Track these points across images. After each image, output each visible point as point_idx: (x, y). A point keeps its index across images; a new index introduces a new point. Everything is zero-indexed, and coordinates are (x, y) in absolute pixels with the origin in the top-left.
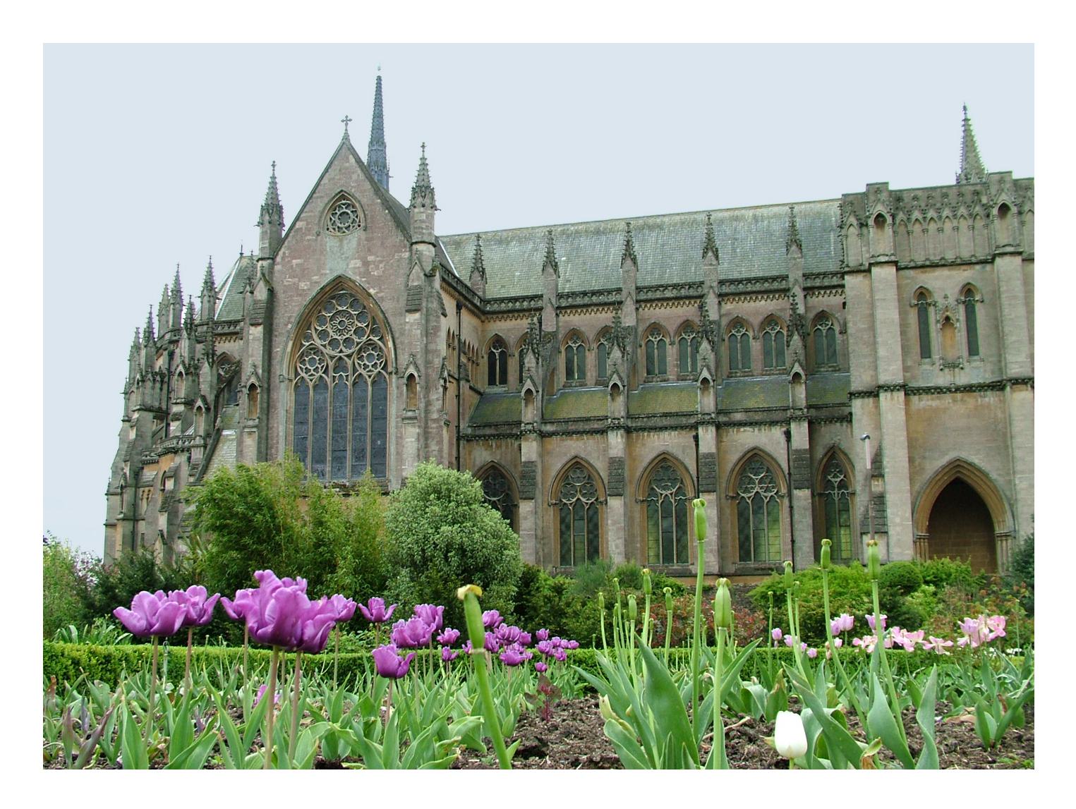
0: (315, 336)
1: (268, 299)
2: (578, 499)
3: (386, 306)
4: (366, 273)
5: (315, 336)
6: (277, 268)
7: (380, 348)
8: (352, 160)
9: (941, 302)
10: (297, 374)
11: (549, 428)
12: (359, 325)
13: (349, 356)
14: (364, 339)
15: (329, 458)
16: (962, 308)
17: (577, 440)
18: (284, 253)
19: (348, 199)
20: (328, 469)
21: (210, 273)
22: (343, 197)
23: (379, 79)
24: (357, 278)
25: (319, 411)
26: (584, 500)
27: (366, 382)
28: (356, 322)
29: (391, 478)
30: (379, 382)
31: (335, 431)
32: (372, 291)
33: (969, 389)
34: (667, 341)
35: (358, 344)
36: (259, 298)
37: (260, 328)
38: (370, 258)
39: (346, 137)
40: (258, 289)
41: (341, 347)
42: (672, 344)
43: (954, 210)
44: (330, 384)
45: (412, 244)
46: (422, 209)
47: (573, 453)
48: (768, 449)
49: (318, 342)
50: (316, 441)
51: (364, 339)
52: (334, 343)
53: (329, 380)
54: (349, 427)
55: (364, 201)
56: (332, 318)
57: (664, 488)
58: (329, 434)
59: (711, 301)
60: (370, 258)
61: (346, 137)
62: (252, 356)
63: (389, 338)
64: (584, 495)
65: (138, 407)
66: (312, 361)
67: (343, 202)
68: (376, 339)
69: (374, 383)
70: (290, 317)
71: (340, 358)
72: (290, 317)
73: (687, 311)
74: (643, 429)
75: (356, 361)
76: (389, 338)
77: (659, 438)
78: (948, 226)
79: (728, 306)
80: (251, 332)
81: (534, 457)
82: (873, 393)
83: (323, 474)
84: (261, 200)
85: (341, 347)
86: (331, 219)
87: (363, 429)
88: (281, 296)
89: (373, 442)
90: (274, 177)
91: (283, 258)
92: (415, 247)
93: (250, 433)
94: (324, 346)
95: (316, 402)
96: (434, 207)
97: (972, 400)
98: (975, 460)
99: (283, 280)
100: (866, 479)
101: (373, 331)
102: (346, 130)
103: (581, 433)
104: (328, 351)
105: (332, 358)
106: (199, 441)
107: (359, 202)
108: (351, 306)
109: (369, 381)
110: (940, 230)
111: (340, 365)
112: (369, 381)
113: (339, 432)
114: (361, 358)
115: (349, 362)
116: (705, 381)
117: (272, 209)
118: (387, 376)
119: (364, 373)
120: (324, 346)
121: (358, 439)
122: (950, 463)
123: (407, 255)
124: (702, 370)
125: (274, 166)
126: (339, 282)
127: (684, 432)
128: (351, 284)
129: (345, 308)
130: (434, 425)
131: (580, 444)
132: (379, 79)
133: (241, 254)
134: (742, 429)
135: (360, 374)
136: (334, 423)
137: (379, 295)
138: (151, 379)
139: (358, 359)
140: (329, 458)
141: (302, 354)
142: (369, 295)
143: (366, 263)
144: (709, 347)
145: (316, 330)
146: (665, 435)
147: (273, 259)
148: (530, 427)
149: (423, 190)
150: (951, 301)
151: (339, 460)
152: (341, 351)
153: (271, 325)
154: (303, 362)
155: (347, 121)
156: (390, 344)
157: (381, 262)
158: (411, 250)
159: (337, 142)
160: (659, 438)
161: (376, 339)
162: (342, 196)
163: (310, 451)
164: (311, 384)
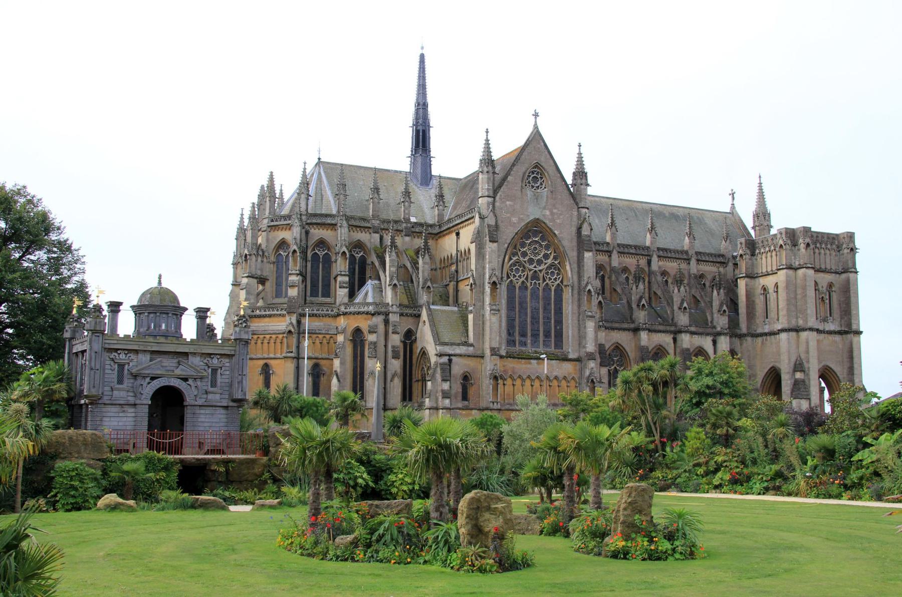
3: (566, 243)
4: (553, 220)
6: (497, 204)
7: (559, 269)
8: (543, 144)
9: (821, 289)
10: (508, 277)
13: (540, 271)
14: (549, 261)
15: (529, 334)
16: (828, 293)
18: (501, 196)
20: (529, 341)
21: (305, 169)
23: (422, 57)
24: (547, 222)
25: (522, 304)
27: (550, 289)
29: (570, 350)
30: (559, 291)
31: (532, 318)
32: (556, 232)
33: (830, 333)
37: (495, 244)
38: (555, 211)
39: (536, 127)
40: (489, 217)
41: (535, 264)
43: (826, 244)
44: (530, 288)
47: (614, 341)
48: (705, 348)
50: (520, 322)
52: (531, 261)
53: (529, 284)
54: (541, 316)
55: (550, 172)
58: (529, 320)
59: (655, 259)
60: (555, 211)
61: (536, 127)
64: (618, 365)
65: (298, 272)
68: (556, 262)
69: (555, 290)
70: (506, 239)
71: (535, 271)
72: (506, 239)
78: (822, 251)
79: (661, 263)
82: (797, 330)
83: (525, 344)
87: (549, 318)
88: (499, 222)
89: (555, 327)
90: (487, 140)
92: (580, 209)
93: (494, 314)
94: (525, 262)
95: (520, 297)
96: (588, 185)
97: (831, 338)
98: (832, 366)
99: (503, 215)
100: (791, 371)
102: (536, 122)
105: (530, 270)
106: (395, 309)
109: (553, 288)
110: (820, 254)
111: (535, 276)
113: (535, 320)
114: (547, 273)
115: (541, 275)
116: (685, 308)
119: (549, 283)
121: (547, 323)
122: (823, 366)
123: (575, 213)
125: (487, 132)
126: (537, 222)
128: (543, 225)
129: (537, 239)
131: (618, 335)
132: (422, 57)
133: (319, 159)
136: (532, 312)
140: (529, 334)
143: (552, 213)
146: (659, 335)
147: (494, 198)
149: (581, 174)
150: (824, 289)
151: (535, 336)
152: (535, 267)
154: (512, 270)
155: (536, 115)
157: (561, 214)
158: (578, 211)
161: (556, 262)
162: (537, 166)
163: (517, 328)
164: (517, 286)
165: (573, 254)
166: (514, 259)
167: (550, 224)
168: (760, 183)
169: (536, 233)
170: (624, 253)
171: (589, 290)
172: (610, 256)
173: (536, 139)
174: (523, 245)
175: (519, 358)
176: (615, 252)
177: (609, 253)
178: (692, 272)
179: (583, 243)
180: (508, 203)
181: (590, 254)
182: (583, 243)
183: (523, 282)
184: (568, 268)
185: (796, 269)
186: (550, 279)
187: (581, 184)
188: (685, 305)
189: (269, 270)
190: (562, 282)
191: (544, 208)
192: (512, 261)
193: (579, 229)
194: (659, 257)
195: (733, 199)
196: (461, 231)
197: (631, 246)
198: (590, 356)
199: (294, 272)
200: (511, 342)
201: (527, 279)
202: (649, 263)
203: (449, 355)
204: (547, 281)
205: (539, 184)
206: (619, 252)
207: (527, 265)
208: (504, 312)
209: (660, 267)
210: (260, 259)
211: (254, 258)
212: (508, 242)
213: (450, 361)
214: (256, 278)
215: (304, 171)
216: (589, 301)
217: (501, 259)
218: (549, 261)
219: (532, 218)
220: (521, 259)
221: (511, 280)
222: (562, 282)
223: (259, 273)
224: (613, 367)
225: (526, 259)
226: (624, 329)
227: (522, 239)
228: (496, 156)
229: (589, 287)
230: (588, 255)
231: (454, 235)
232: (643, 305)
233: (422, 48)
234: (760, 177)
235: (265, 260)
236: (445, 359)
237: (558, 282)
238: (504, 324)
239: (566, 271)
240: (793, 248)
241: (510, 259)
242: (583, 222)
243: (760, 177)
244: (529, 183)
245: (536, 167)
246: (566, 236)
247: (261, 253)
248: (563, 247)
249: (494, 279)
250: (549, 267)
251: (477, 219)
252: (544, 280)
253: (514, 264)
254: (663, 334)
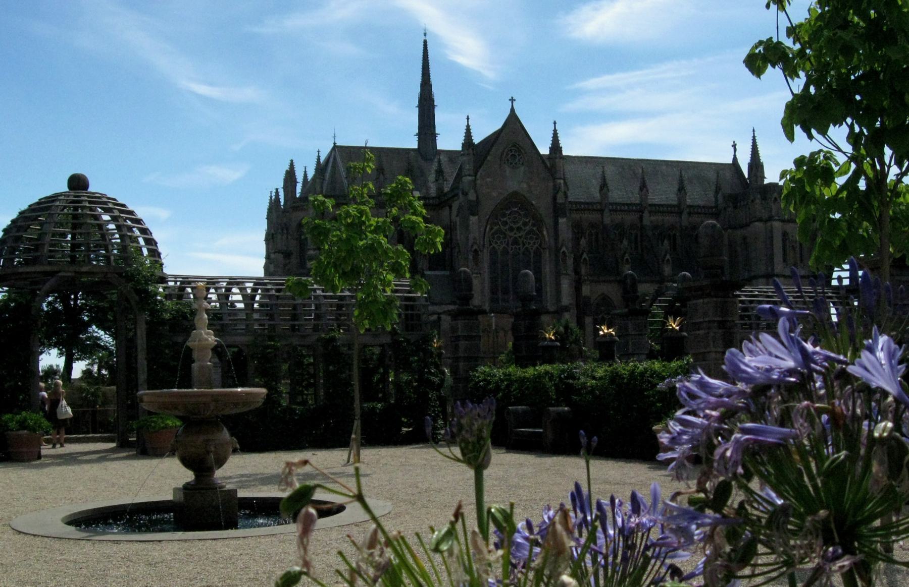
6: (478, 182)
10: (491, 244)
14: (528, 228)
23: (425, 42)
32: (534, 202)
39: (512, 110)
41: (515, 231)
52: (511, 229)
53: (509, 249)
59: (646, 215)
61: (512, 110)
66: (499, 238)
68: (535, 228)
71: (516, 238)
73: (634, 217)
79: (653, 218)
90: (468, 126)
93: (476, 278)
101: (534, 225)
102: (512, 106)
103: (604, 281)
104: (508, 233)
105: (510, 237)
109: (532, 252)
112: (532, 252)
115: (520, 240)
118: (542, 250)
123: (551, 184)
125: (468, 119)
126: (515, 194)
129: (516, 209)
132: (425, 42)
133: (335, 144)
142: (532, 204)
147: (475, 176)
149: (556, 147)
155: (512, 100)
159: (507, 113)
161: (535, 228)
165: (549, 221)
166: (496, 228)
167: (527, 195)
168: (754, 137)
170: (616, 211)
171: (564, 252)
172: (602, 215)
173: (513, 123)
174: (504, 215)
175: (501, 313)
176: (607, 210)
177: (601, 211)
178: (683, 224)
179: (558, 210)
181: (565, 220)
182: (558, 210)
183: (504, 247)
184: (545, 233)
185: (766, 221)
186: (529, 243)
187: (556, 158)
188: (668, 257)
189: (293, 246)
192: (492, 231)
193: (555, 198)
194: (650, 212)
195: (735, 150)
196: (453, 205)
197: (623, 204)
198: (566, 309)
199: (312, 247)
200: (494, 300)
201: (508, 245)
202: (641, 218)
203: (439, 314)
204: (527, 246)
205: (517, 160)
206: (610, 211)
207: (508, 233)
208: (486, 276)
209: (651, 222)
210: (285, 236)
211: (279, 236)
212: (489, 213)
213: (439, 318)
214: (282, 253)
215: (319, 159)
216: (564, 261)
217: (482, 229)
218: (528, 228)
219: (510, 191)
220: (502, 227)
221: (494, 247)
222: (540, 245)
223: (285, 248)
224: (600, 316)
225: (507, 227)
226: (610, 282)
227: (502, 209)
228: (477, 139)
229: (564, 249)
230: (562, 220)
231: (447, 208)
232: (627, 259)
233: (425, 34)
234: (754, 131)
235: (289, 237)
236: (435, 317)
237: (537, 245)
238: (487, 285)
239: (543, 236)
240: (763, 202)
241: (491, 229)
242: (558, 192)
243: (754, 131)
244: (508, 160)
245: (514, 146)
246: (543, 206)
247: (285, 231)
248: (541, 215)
249: (475, 247)
250: (528, 233)
251: (460, 194)
252: (524, 245)
253: (496, 233)
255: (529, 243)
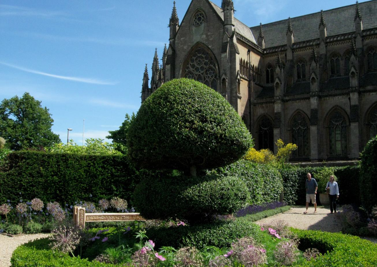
0: (190, 67)
1: (172, 55)
2: (300, 128)
5: (190, 67)
6: (176, 42)
11: (287, 98)
12: (206, 61)
13: (202, 74)
14: (208, 66)
17: (299, 102)
18: (178, 36)
19: (200, 12)
22: (198, 11)
26: (302, 128)
28: (205, 60)
32: (210, 47)
34: (340, 58)
35: (206, 68)
36: (169, 54)
37: (169, 66)
38: (209, 34)
42: (342, 60)
45: (224, 26)
46: (227, 11)
49: (191, 69)
51: (208, 66)
52: (197, 69)
56: (196, 59)
57: (336, 121)
60: (209, 34)
62: (167, 76)
63: (216, 65)
67: (199, 13)
74: (326, 96)
75: (205, 75)
76: (216, 65)
77: (333, 100)
79: (367, 41)
80: (166, 67)
81: (280, 110)
84: (170, 16)
85: (200, 70)
86: (195, 20)
88: (177, 52)
90: (174, 8)
91: (178, 38)
92: (225, 26)
94: (194, 71)
101: (211, 63)
105: (196, 75)
107: (204, 11)
108: (203, 54)
114: (207, 74)
117: (173, 20)
120: (194, 71)
124: (351, 68)
125: (174, 3)
127: (344, 97)
130: (234, 99)
134: (371, 94)
135: (207, 80)
137: (213, 48)
138: (147, 91)
139: (206, 74)
141: (186, 74)
142: (209, 48)
143: (207, 36)
144: (355, 58)
145: (190, 65)
148: (278, 98)
152: (200, 72)
153: (174, 64)
156: (217, 67)
157: (213, 34)
160: (333, 100)
169: (199, 51)
174: (192, 61)
180: (182, 39)
190: (216, 77)
191: (202, 34)
219: (195, 42)
232: (313, 78)
254: (340, 97)
255: (209, 77)
